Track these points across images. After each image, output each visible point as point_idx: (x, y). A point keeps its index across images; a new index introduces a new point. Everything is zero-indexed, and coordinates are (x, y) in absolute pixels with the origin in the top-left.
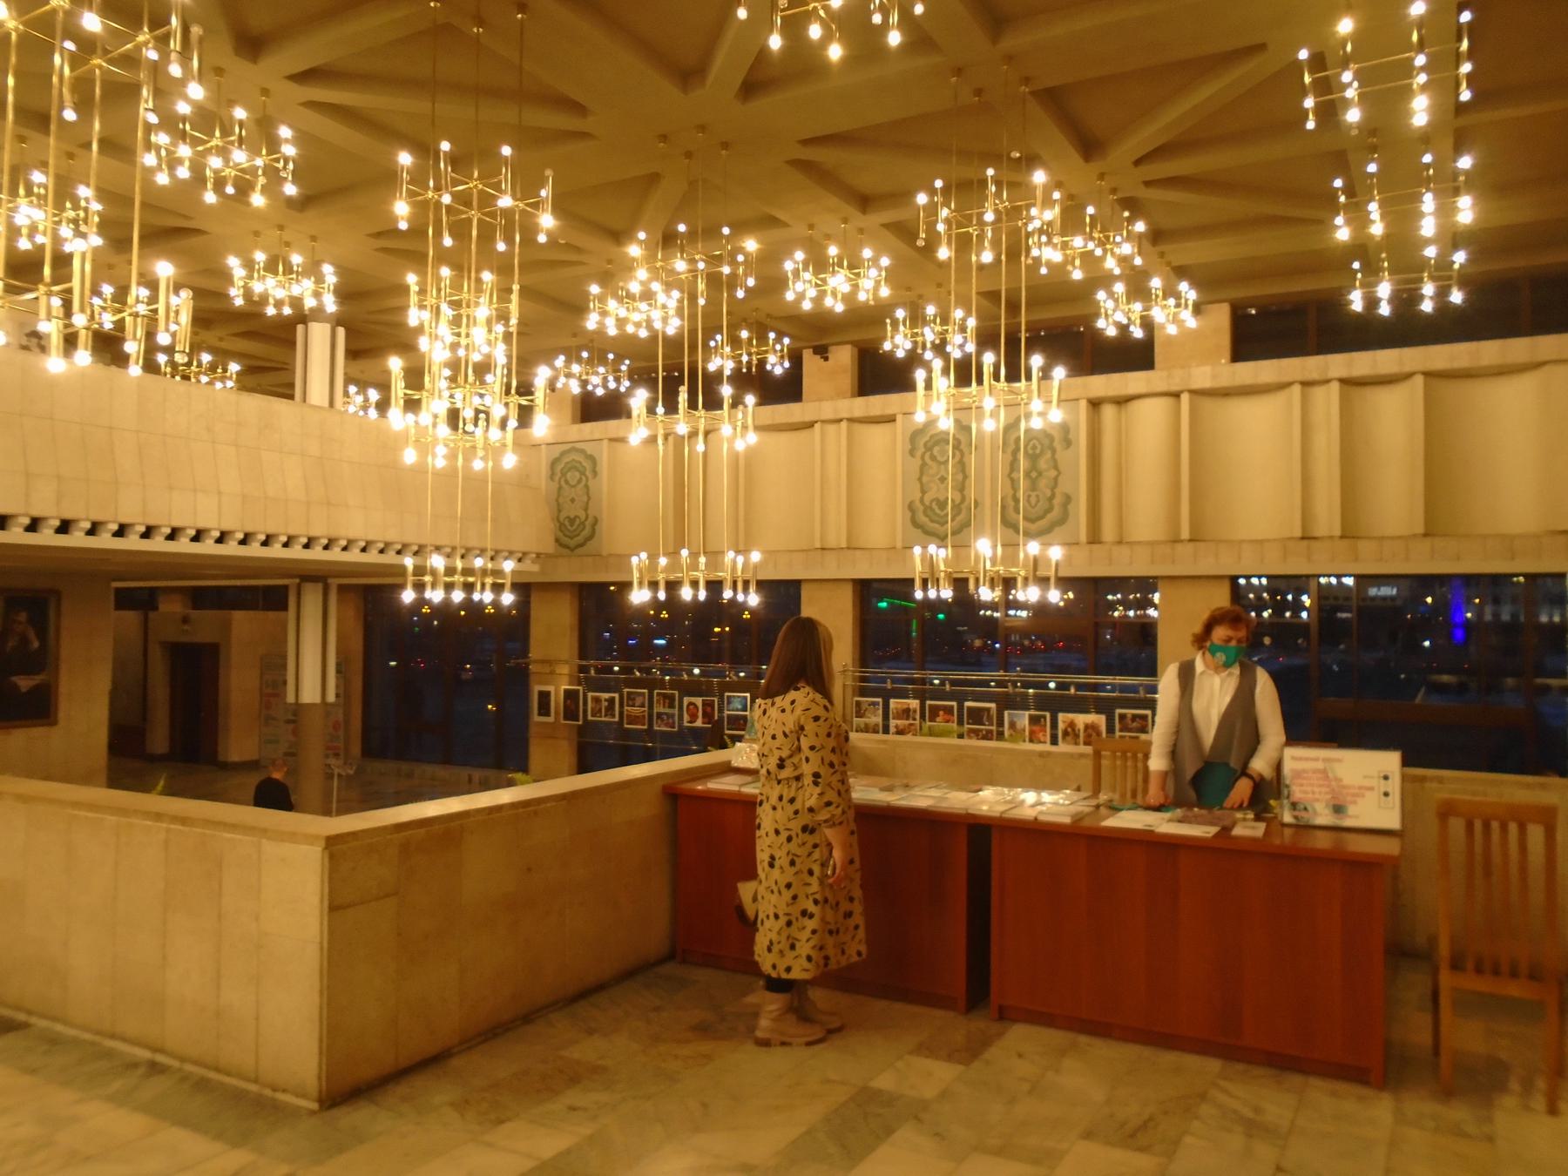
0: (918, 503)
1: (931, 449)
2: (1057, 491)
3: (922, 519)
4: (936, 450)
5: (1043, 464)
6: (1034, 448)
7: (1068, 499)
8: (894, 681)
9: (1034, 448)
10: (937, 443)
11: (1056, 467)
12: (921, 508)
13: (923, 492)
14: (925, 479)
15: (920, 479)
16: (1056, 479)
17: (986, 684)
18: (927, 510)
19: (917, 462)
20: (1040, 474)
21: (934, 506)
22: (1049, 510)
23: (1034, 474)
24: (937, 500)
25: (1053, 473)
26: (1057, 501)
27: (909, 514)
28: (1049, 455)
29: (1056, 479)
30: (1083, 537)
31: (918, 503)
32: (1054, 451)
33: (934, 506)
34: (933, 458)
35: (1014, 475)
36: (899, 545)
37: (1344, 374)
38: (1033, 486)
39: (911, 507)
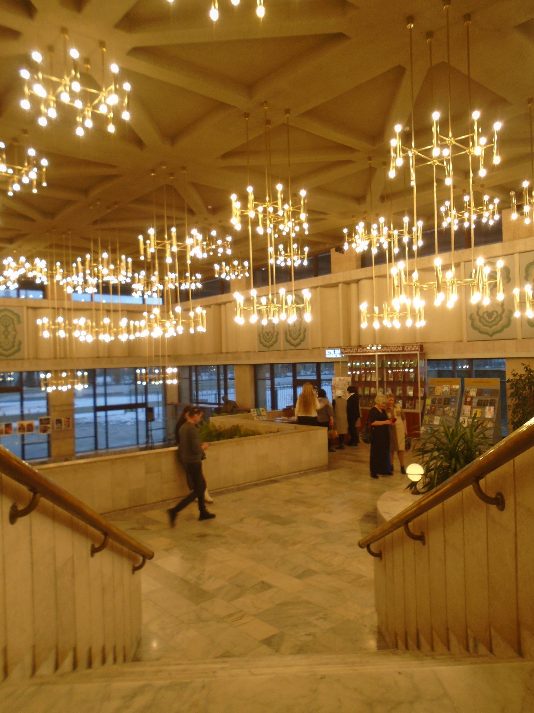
0: (476, 315)
3: (478, 323)
12: (478, 318)
21: (485, 316)
27: (470, 322)
33: (485, 316)
36: (465, 339)
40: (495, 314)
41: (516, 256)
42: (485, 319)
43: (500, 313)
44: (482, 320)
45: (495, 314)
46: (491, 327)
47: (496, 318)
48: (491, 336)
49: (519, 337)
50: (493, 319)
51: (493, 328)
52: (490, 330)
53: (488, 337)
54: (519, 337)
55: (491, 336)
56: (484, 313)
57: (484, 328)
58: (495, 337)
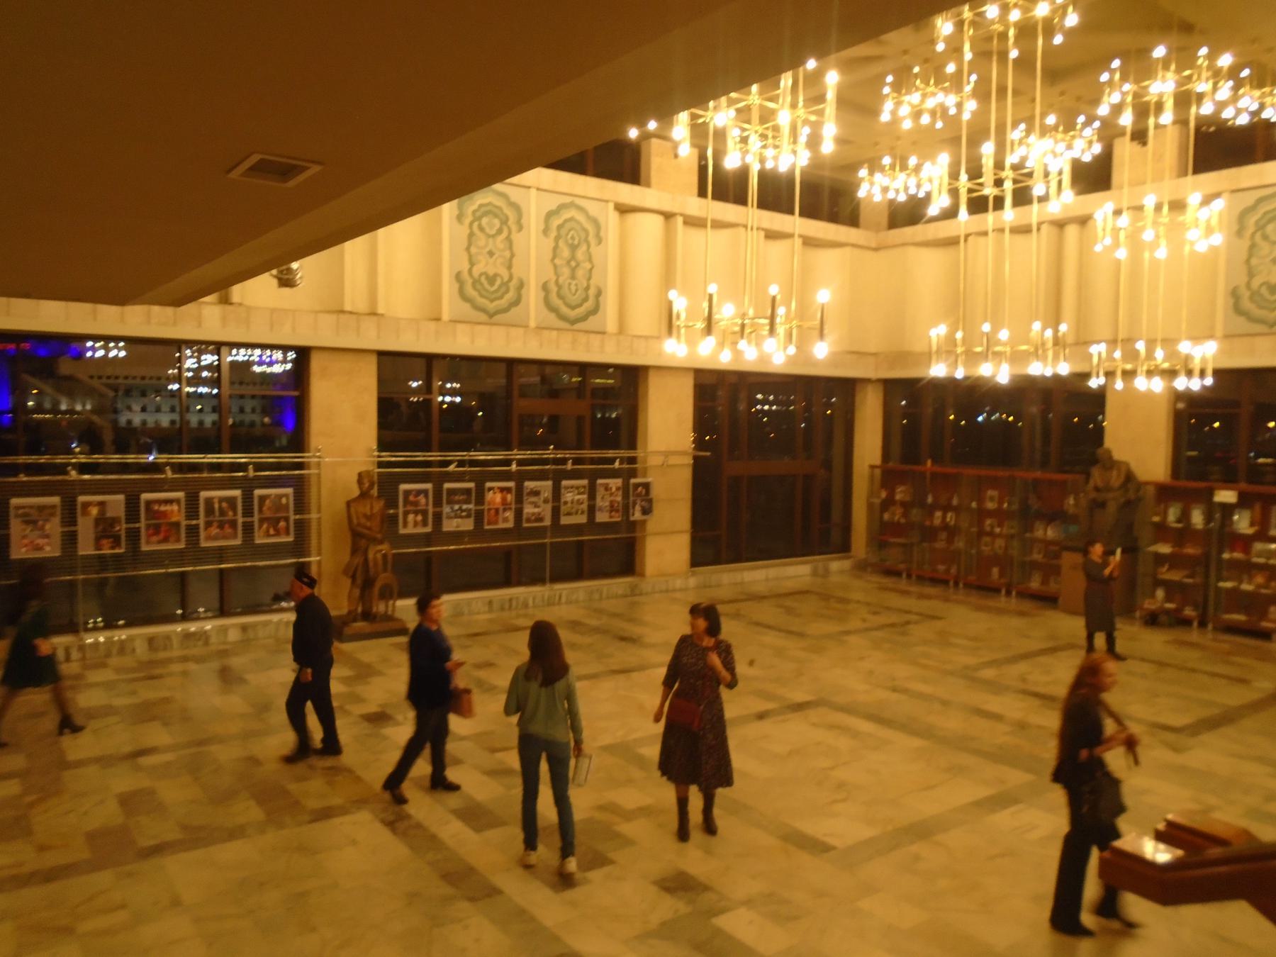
1: (480, 218)
2: (592, 282)
4: (485, 221)
5: (580, 254)
6: (573, 238)
7: (599, 293)
8: (577, 461)
9: (573, 238)
10: (486, 214)
11: (590, 260)
12: (470, 281)
13: (472, 264)
14: (473, 250)
15: (468, 249)
16: (591, 270)
17: (612, 461)
18: (476, 283)
19: (465, 230)
20: (578, 265)
21: (483, 279)
22: (586, 299)
23: (573, 264)
24: (485, 273)
25: (588, 266)
26: (592, 292)
27: (457, 286)
28: (584, 248)
29: (591, 270)
30: (611, 326)
31: (465, 275)
32: (589, 247)
34: (481, 229)
35: (557, 261)
37: (766, 225)
38: (573, 277)
39: (458, 277)
40: (498, 282)
41: (533, 191)
42: (482, 284)
43: (506, 279)
44: (479, 287)
45: (498, 282)
46: (492, 301)
47: (500, 287)
48: (491, 316)
49: (532, 324)
50: (495, 287)
51: (497, 302)
52: (491, 306)
53: (483, 317)
54: (532, 324)
55: (491, 316)
56: (481, 275)
57: (482, 301)
58: (497, 318)
